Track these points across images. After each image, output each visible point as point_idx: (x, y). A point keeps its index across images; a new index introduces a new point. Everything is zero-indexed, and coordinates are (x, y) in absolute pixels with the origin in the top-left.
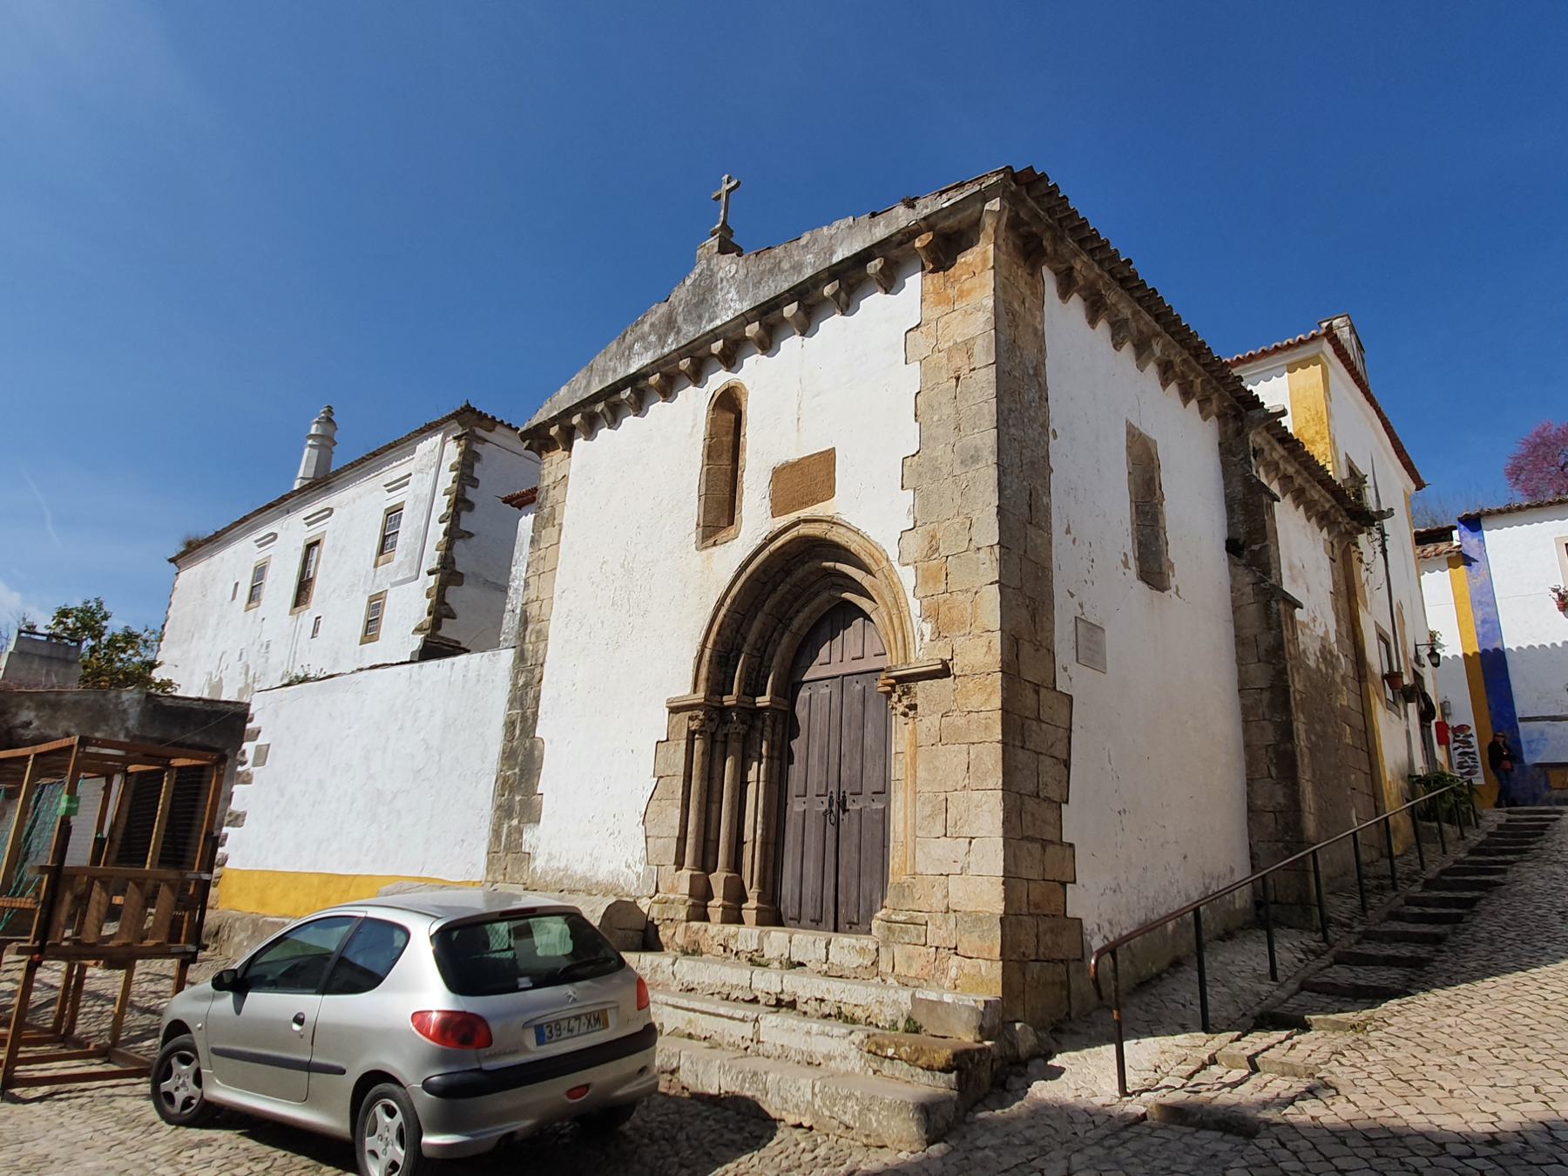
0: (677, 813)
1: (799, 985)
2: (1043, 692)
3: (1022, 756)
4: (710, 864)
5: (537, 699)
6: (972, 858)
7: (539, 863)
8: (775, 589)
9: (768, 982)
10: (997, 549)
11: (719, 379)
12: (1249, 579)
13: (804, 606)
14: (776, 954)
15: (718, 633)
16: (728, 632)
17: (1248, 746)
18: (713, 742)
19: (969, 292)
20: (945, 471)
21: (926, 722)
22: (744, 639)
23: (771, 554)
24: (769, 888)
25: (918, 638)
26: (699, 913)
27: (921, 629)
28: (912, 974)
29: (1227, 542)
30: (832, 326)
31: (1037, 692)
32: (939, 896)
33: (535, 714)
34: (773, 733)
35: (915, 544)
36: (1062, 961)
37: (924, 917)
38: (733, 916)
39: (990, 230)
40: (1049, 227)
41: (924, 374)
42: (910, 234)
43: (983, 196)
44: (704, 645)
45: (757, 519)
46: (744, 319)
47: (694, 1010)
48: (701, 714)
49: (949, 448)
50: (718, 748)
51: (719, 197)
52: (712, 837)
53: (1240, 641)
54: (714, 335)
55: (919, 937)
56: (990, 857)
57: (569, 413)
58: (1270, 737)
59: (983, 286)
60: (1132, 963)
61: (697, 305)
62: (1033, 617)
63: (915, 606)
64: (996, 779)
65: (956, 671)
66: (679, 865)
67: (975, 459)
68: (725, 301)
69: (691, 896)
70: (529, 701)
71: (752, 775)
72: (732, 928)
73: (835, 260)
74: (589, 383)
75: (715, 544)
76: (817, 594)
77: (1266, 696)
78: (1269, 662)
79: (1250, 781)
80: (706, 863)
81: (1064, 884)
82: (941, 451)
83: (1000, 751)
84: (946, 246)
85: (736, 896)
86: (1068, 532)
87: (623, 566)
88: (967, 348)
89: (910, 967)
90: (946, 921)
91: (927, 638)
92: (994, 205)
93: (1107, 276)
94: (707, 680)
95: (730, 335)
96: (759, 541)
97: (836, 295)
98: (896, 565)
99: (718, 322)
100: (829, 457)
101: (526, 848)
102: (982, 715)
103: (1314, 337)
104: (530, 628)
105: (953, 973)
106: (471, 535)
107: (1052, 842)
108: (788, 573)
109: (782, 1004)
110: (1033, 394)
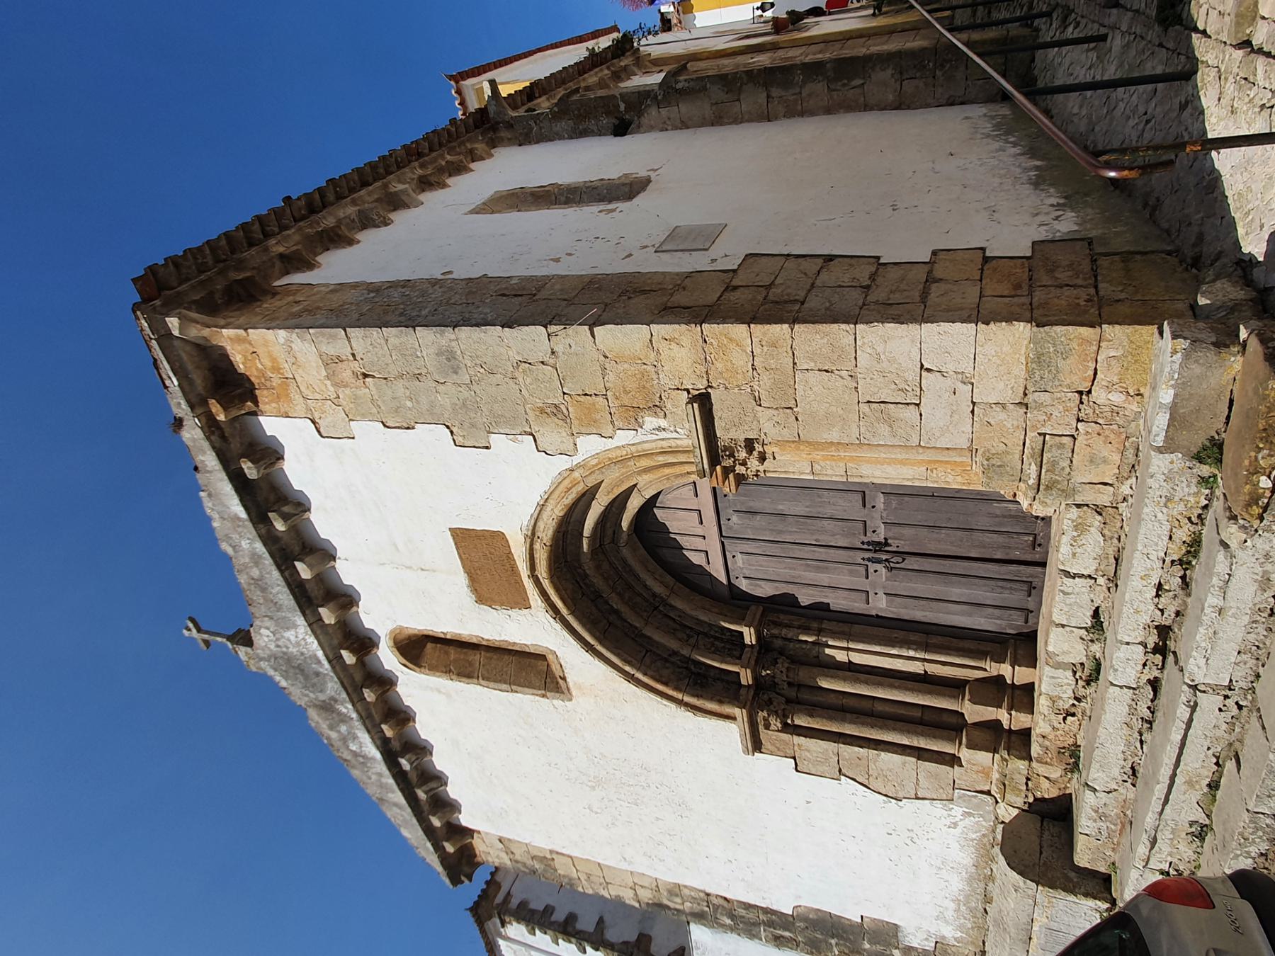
0: (888, 759)
1: (1134, 616)
2: (735, 282)
3: (814, 302)
4: (953, 720)
5: (748, 906)
6: (949, 368)
7: (950, 933)
8: (617, 612)
9: (1126, 663)
10: (552, 328)
11: (388, 658)
12: (653, 111)
13: (638, 578)
14: (1081, 647)
15: (666, 684)
16: (665, 672)
17: (828, 111)
18: (798, 702)
19: (274, 360)
20: (466, 394)
21: (767, 427)
22: (675, 653)
23: (572, 613)
24: (984, 647)
25: (663, 435)
26: (1020, 742)
28: (1116, 458)
29: (616, 134)
30: (324, 522)
31: (736, 288)
32: (1002, 416)
33: (767, 911)
34: (788, 626)
35: (552, 435)
36: (1094, 261)
37: (1033, 439)
38: (1024, 697)
39: (206, 332)
40: (221, 272)
41: (365, 417)
42: (211, 427)
43: (165, 337)
44: (680, 703)
45: (534, 627)
46: (315, 624)
47: (1174, 775)
48: (762, 714)
49: (441, 387)
50: (805, 695)
51: (207, 643)
52: (917, 714)
53: (718, 120)
54: (335, 660)
55: (1061, 446)
56: (948, 341)
57: (429, 831)
58: (819, 87)
59: (266, 343)
60: (1086, 195)
61: (306, 677)
62: (643, 292)
64: (841, 332)
65: (701, 385)
66: (953, 761)
67: (450, 356)
68: (298, 644)
69: (995, 751)
70: (751, 915)
71: (841, 656)
72: (1042, 703)
73: (243, 514)
74: (396, 805)
75: (564, 679)
76: (624, 561)
77: (775, 92)
78: (740, 89)
79: (867, 108)
80: (951, 726)
81: (986, 260)
82: (446, 398)
83: (803, 326)
84: (227, 387)
85: (995, 690)
86: (557, 260)
87: (593, 788)
88: (331, 362)
89: (1105, 461)
90: (1039, 406)
91: (663, 423)
92: (173, 323)
93: (301, 224)
94: (721, 702)
95: (336, 642)
96: (558, 626)
97: (285, 517)
98: (577, 459)
99: (320, 654)
100: (465, 539)
101: (930, 946)
103: (459, 92)
104: (666, 902)
105: (1117, 398)
106: (601, 921)
107: (930, 272)
108: (597, 596)
109: (1162, 644)
110: (396, 294)
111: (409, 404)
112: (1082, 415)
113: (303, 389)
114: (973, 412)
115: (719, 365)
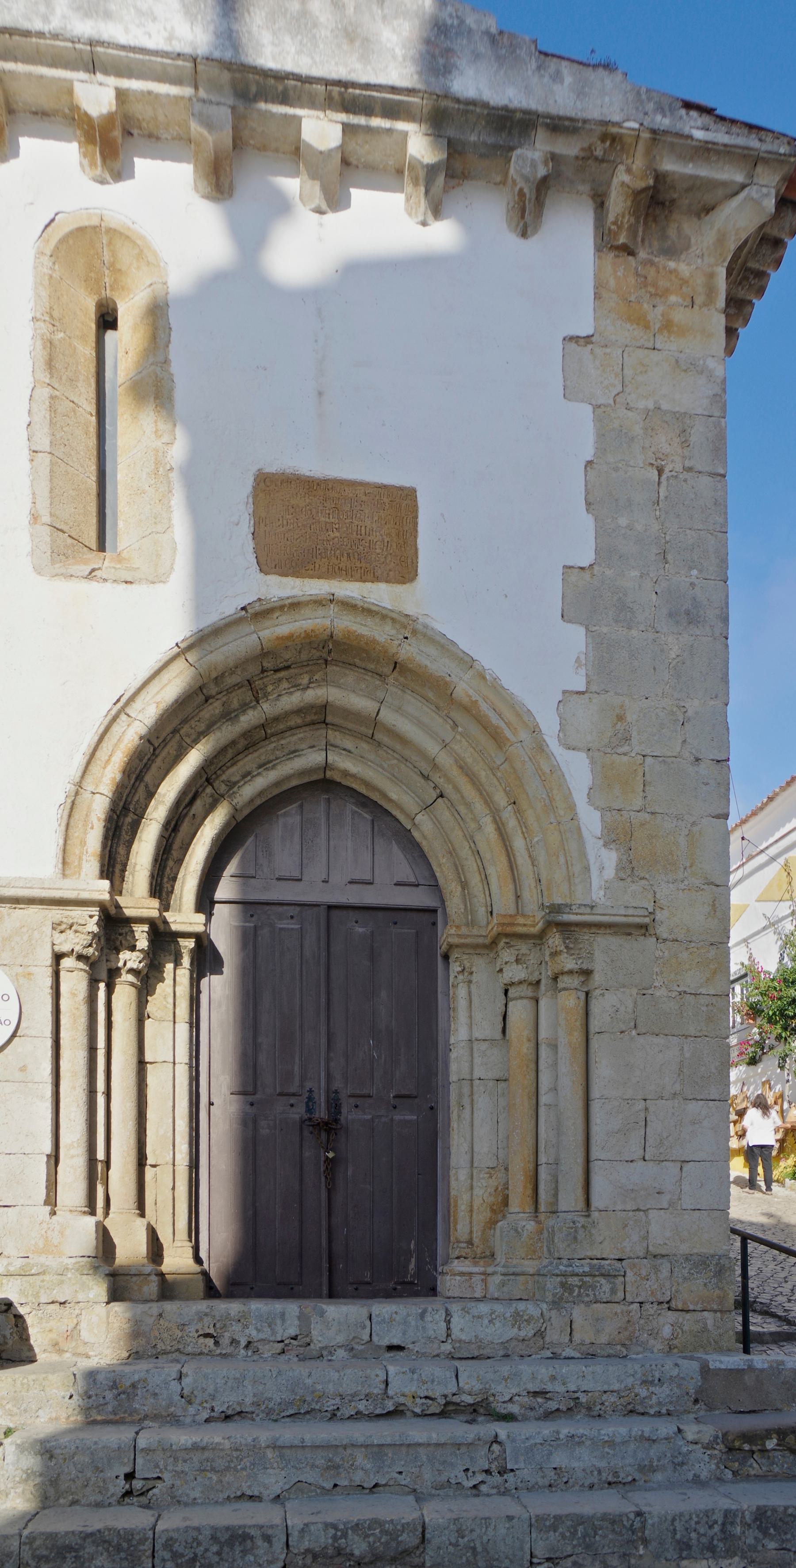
27: (604, 862)
41: (601, 436)
63: (591, 821)
65: (663, 931)
90: (656, 1269)
91: (610, 872)
102: (703, 1000)
111: (623, 521)
112: (647, 1306)
113: (640, 353)
114: (638, 1210)
115: (685, 955)
